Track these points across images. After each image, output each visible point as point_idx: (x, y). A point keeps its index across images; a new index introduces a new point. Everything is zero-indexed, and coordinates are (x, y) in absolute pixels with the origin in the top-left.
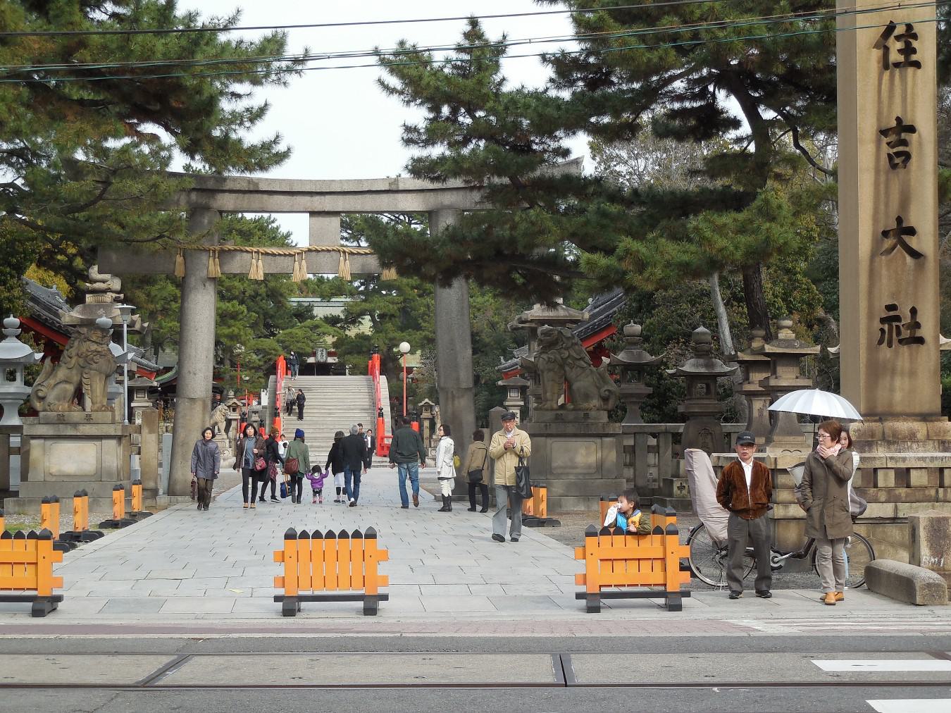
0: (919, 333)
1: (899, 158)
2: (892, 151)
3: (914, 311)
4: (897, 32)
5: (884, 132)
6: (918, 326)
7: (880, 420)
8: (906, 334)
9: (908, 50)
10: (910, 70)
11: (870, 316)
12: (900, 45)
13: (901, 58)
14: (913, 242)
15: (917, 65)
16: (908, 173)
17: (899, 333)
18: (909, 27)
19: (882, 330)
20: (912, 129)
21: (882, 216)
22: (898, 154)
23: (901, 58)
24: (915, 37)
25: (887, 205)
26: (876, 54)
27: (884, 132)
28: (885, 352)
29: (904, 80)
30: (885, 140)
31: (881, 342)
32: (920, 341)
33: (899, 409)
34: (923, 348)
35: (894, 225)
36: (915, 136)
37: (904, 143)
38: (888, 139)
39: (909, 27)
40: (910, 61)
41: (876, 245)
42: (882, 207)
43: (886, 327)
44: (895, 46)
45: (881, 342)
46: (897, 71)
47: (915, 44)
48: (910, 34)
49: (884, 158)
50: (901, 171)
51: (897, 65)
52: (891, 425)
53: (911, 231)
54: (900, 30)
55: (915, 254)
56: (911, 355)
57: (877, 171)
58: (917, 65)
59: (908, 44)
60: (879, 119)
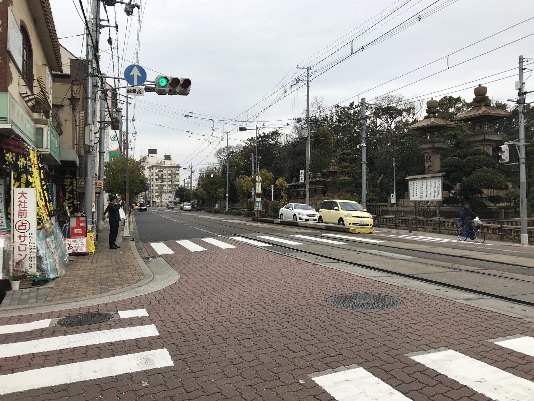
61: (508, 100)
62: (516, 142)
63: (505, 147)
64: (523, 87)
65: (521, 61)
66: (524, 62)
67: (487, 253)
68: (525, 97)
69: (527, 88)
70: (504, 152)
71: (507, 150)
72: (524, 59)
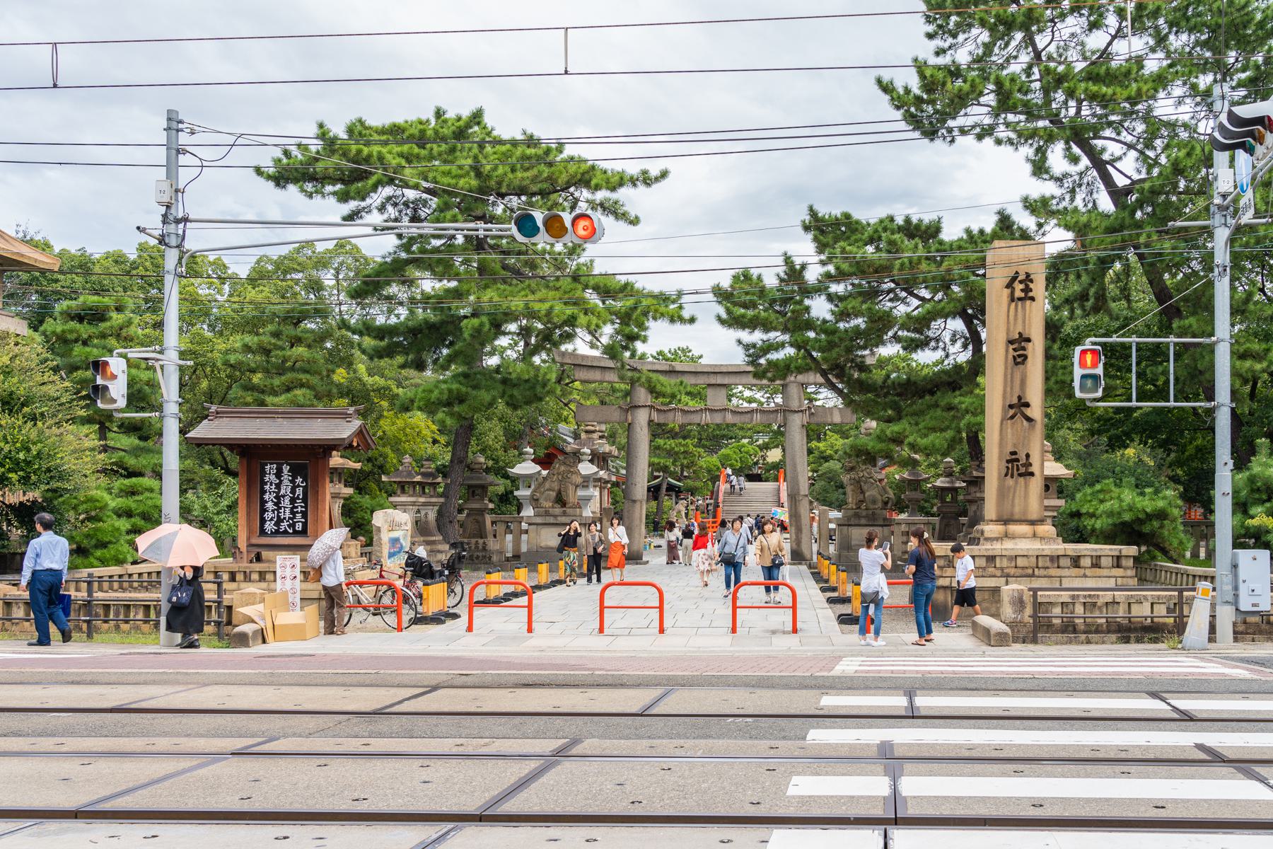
0: (1031, 469)
1: (1020, 359)
2: (1016, 354)
3: (1028, 456)
4: (1019, 278)
5: (1011, 342)
6: (1031, 465)
7: (1005, 524)
8: (1023, 470)
9: (1027, 290)
10: (1028, 302)
11: (1000, 459)
12: (1022, 286)
13: (1022, 295)
14: (1028, 412)
15: (1033, 299)
16: (1026, 368)
17: (1018, 470)
18: (1028, 275)
19: (1008, 467)
20: (1028, 340)
21: (1008, 395)
22: (1019, 356)
23: (1022, 295)
24: (1031, 281)
25: (1012, 388)
26: (1007, 292)
27: (1011, 342)
28: (1010, 482)
29: (1024, 308)
30: (1011, 347)
31: (1006, 475)
32: (1032, 474)
33: (1017, 517)
34: (1033, 479)
35: (1015, 401)
36: (1030, 344)
37: (1024, 349)
38: (1014, 346)
39: (1028, 275)
40: (1028, 296)
41: (1004, 412)
42: (1008, 389)
43: (1010, 465)
44: (1019, 287)
45: (1006, 475)
46: (1020, 303)
47: (1031, 286)
48: (1028, 279)
49: (1010, 357)
50: (1021, 367)
51: (1020, 299)
52: (1014, 528)
53: (1027, 405)
54: (1022, 277)
55: (1029, 420)
56: (1026, 483)
57: (1006, 368)
58: (1033, 299)
59: (1027, 286)
60: (1007, 334)
61: (138, 228)
62: (154, 351)
63: (116, 365)
64: (177, 200)
65: (174, 125)
66: (182, 131)
67: (190, 686)
68: (184, 231)
69: (190, 205)
70: (114, 377)
71: (123, 372)
72: (181, 122)
